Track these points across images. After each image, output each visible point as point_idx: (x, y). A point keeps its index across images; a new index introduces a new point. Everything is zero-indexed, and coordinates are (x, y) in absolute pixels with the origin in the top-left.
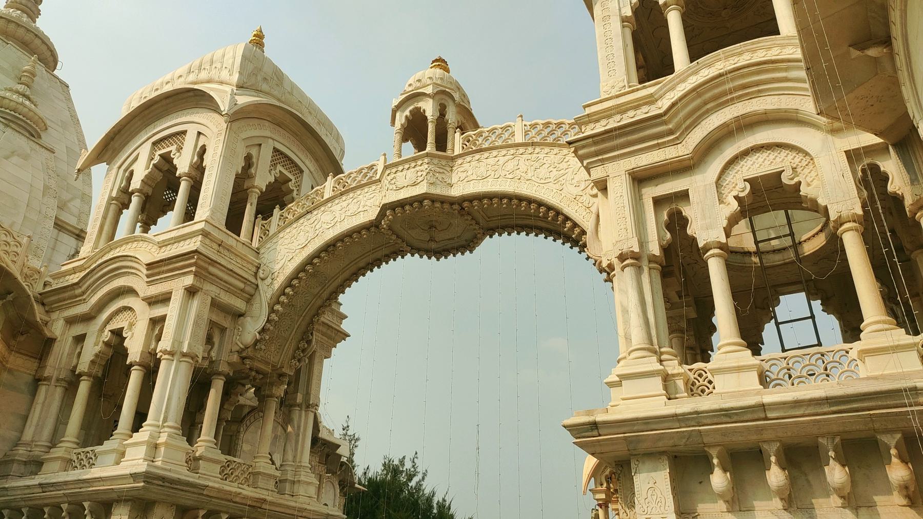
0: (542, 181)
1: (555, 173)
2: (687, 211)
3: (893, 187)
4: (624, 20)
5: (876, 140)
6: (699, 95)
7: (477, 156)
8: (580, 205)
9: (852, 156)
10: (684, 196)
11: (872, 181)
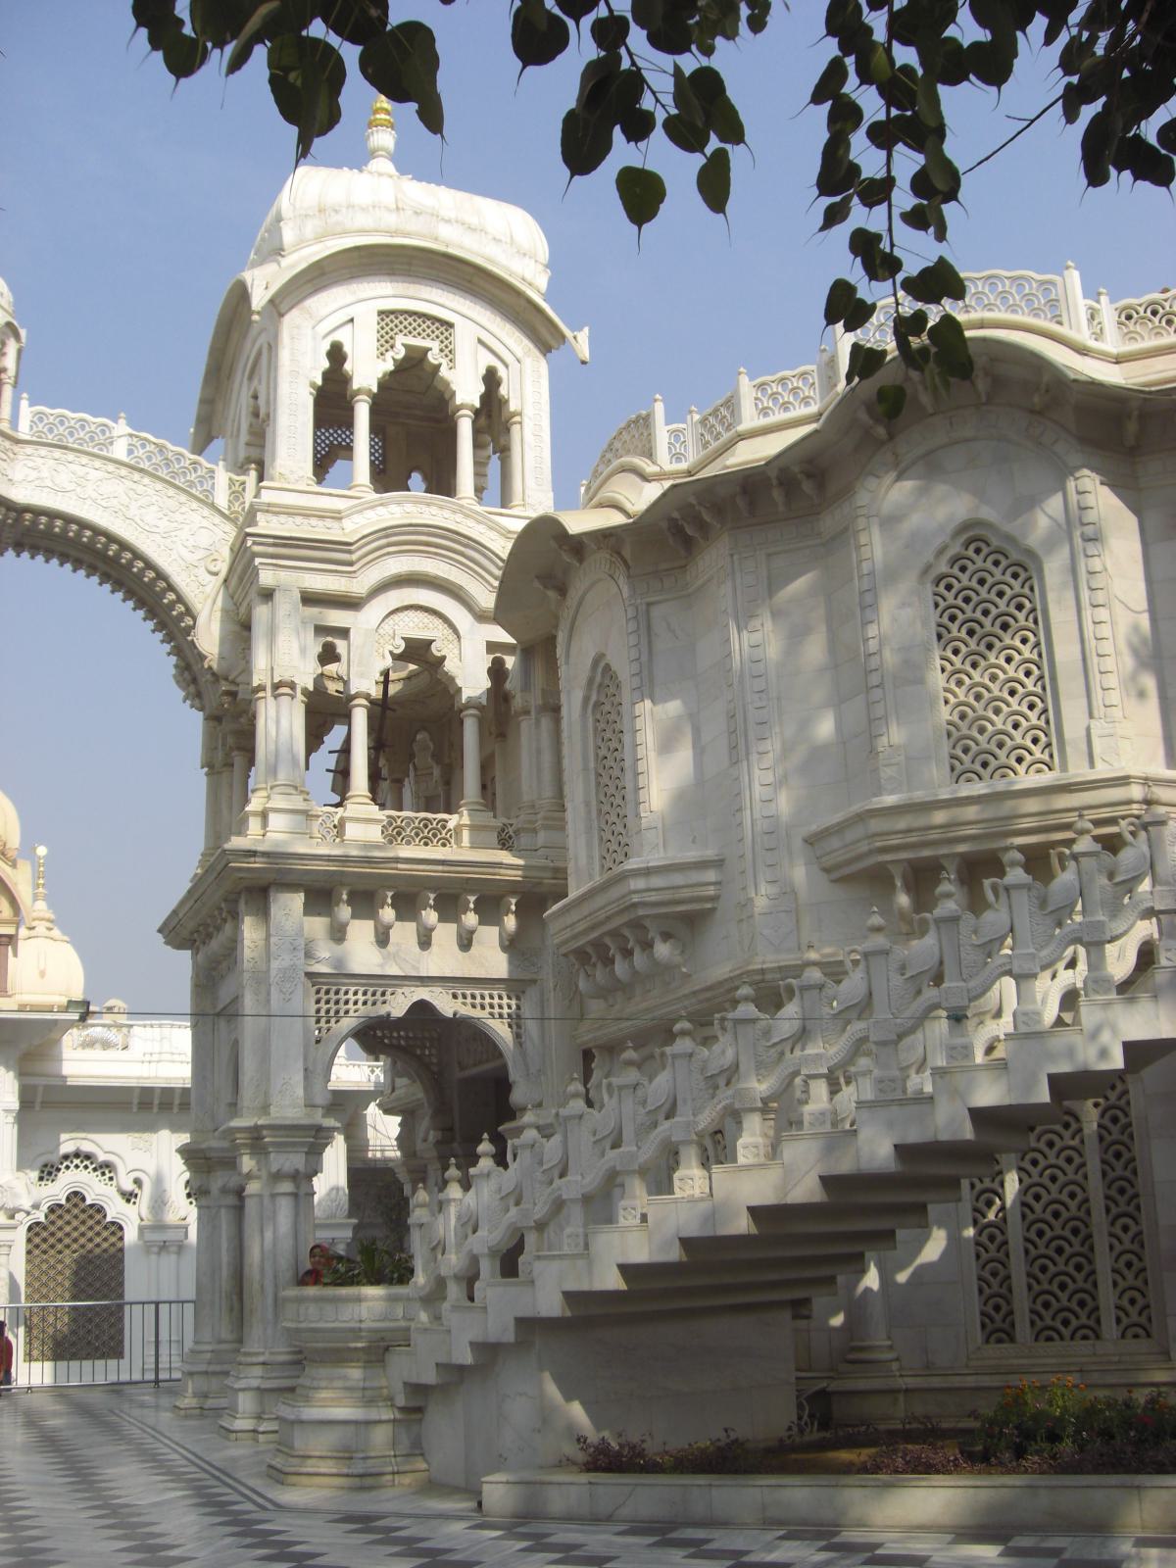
0: (147, 528)
1: (164, 524)
2: (341, 646)
3: (508, 686)
4: (313, 385)
5: (509, 639)
6: (387, 536)
7: (57, 453)
8: (193, 578)
9: (491, 647)
10: (344, 633)
11: (497, 672)
